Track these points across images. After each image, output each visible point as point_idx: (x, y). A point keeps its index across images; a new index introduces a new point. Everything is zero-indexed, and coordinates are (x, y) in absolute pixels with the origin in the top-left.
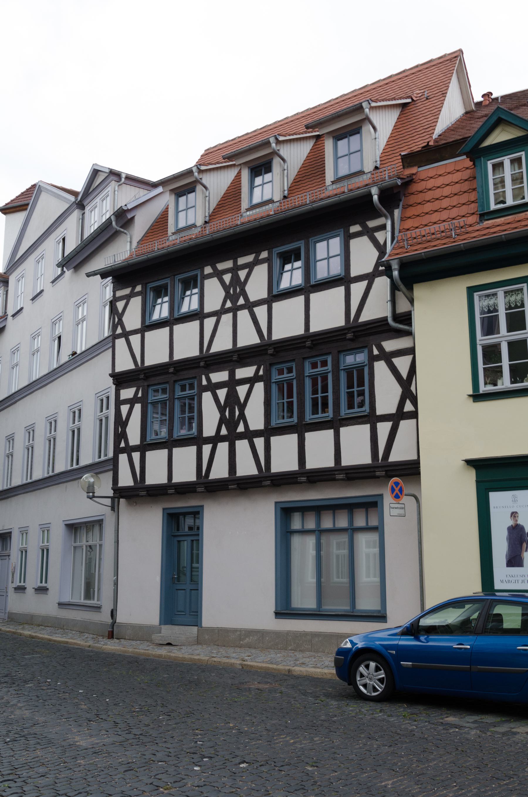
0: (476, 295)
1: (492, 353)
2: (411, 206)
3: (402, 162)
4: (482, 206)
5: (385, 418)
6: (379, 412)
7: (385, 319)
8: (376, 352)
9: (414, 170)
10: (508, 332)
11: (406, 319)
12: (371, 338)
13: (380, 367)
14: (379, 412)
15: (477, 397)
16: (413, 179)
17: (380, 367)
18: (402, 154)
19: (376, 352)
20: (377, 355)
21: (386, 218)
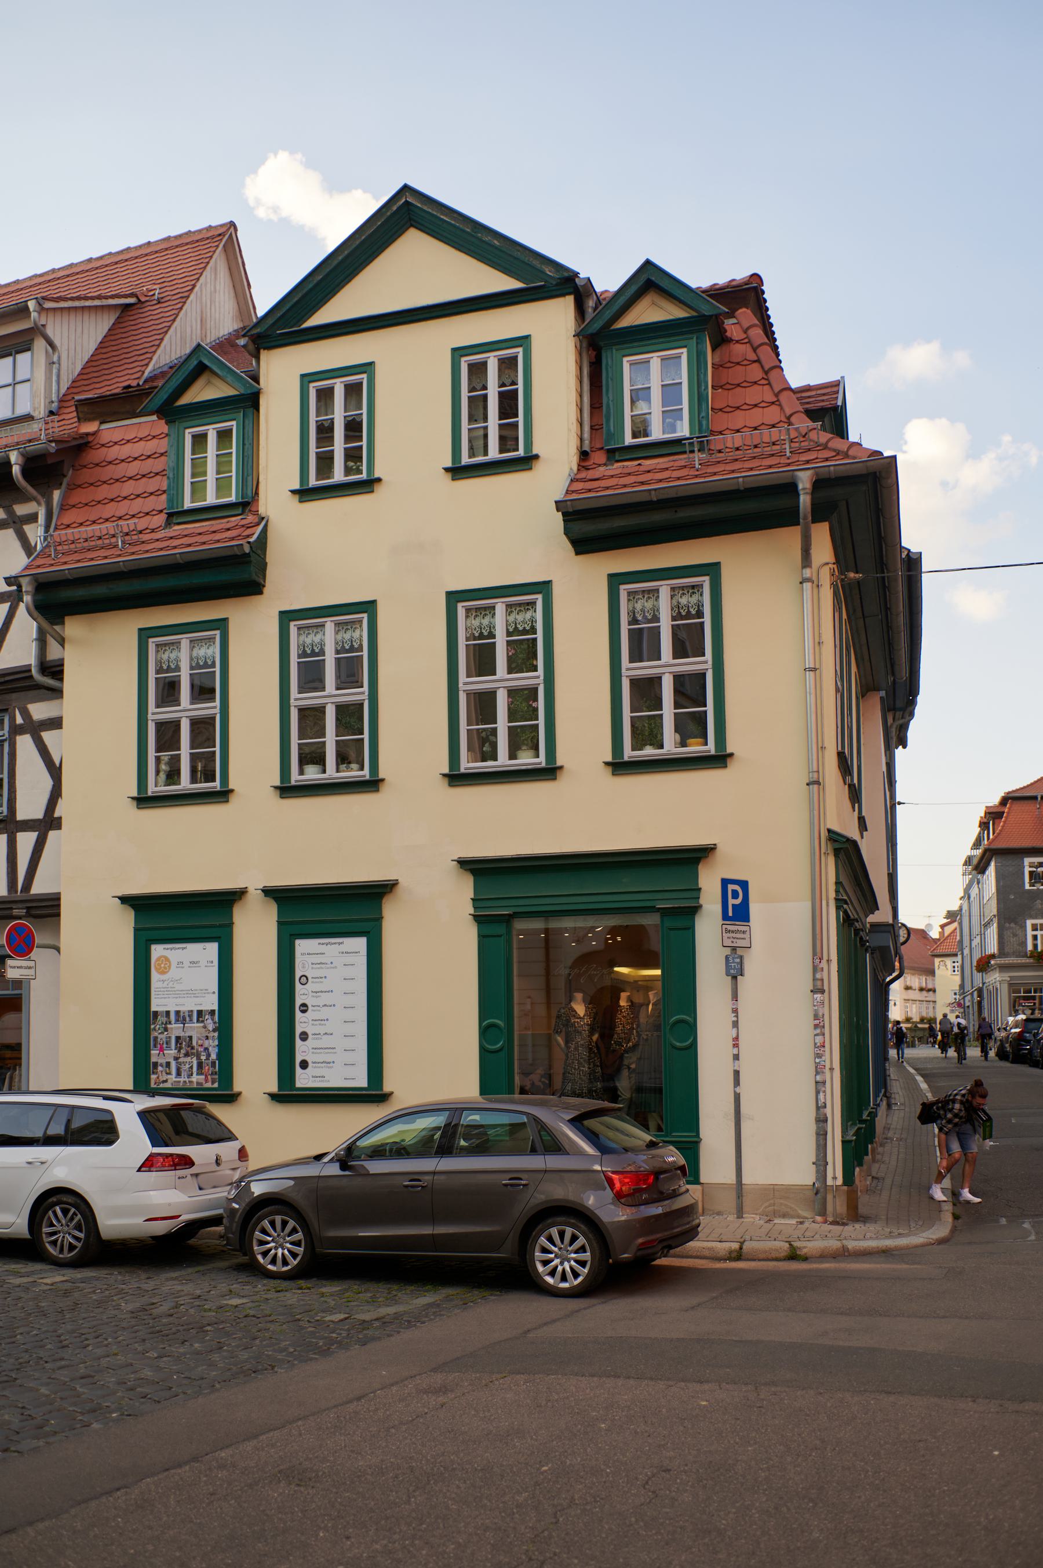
0: (152, 642)
1: (168, 735)
2: (79, 486)
3: (77, 410)
4: (170, 501)
5: (27, 825)
6: (20, 816)
7: (27, 669)
8: (19, 720)
9: (90, 427)
10: (192, 703)
11: (54, 670)
12: (14, 696)
13: (25, 743)
14: (20, 816)
15: (144, 801)
16: (89, 442)
17: (25, 743)
18: (77, 397)
19: (19, 720)
20: (21, 725)
21: (39, 504)
